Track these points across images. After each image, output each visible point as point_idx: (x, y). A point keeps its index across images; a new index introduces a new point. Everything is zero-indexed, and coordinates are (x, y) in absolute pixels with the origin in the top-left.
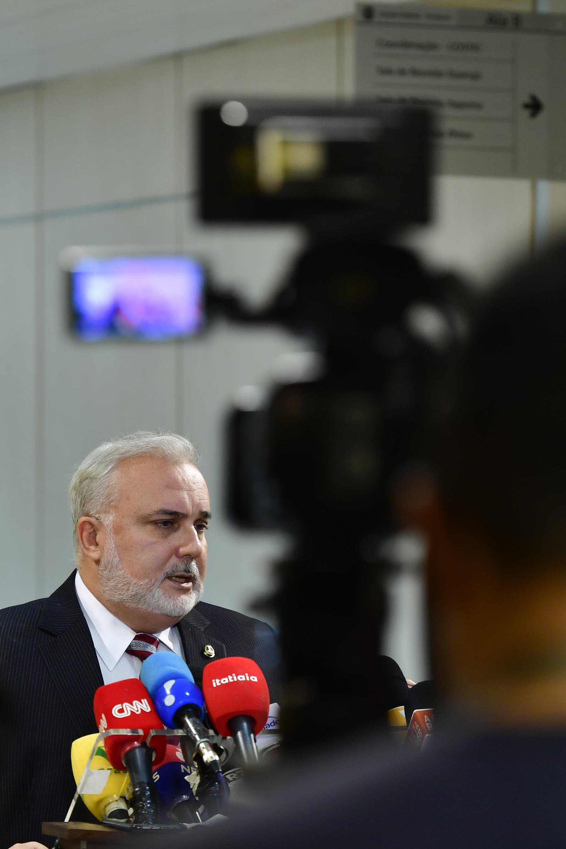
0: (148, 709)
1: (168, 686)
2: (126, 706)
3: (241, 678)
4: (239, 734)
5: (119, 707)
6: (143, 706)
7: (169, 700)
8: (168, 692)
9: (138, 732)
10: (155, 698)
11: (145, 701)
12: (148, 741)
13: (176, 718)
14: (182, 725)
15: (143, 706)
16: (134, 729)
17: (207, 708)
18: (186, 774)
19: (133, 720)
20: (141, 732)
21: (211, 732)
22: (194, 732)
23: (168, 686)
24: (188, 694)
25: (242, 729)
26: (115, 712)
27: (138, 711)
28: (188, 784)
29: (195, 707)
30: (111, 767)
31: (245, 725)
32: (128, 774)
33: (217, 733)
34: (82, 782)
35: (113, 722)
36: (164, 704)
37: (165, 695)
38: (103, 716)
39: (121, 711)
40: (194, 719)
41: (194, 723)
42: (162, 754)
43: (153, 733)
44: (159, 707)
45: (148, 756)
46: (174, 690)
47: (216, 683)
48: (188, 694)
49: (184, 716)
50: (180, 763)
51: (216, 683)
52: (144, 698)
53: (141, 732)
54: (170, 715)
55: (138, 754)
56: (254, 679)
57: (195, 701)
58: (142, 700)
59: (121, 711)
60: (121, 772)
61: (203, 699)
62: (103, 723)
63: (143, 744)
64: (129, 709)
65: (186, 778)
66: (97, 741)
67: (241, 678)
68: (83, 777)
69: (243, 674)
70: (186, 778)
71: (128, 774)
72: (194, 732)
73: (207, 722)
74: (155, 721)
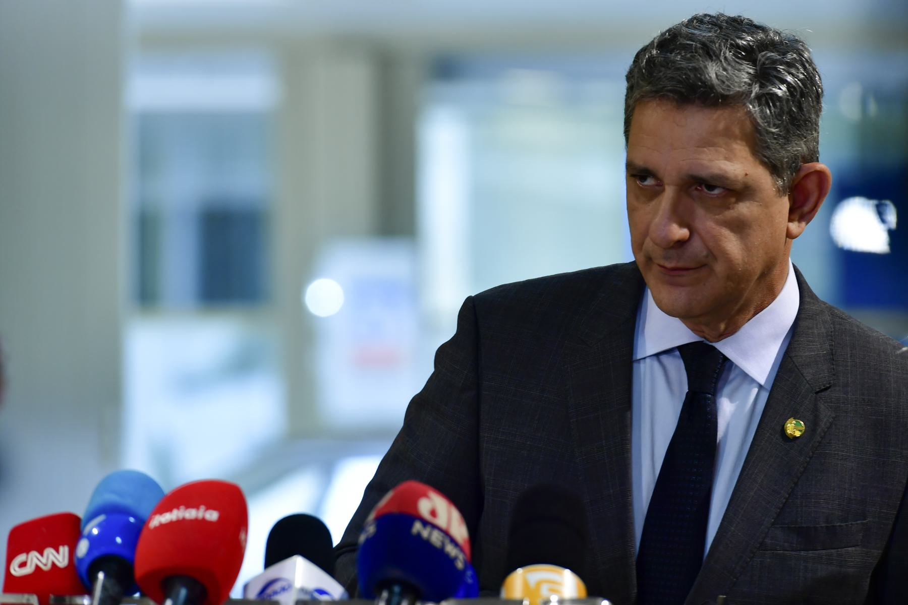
2: (34, 554)
3: (191, 514)
5: (21, 558)
11: (64, 550)
24: (119, 540)
27: (45, 565)
31: (183, 592)
39: (23, 565)
41: (104, 587)
48: (119, 540)
52: (63, 545)
56: (212, 516)
58: (61, 549)
59: (23, 565)
64: (35, 561)
67: (191, 514)
69: (197, 507)
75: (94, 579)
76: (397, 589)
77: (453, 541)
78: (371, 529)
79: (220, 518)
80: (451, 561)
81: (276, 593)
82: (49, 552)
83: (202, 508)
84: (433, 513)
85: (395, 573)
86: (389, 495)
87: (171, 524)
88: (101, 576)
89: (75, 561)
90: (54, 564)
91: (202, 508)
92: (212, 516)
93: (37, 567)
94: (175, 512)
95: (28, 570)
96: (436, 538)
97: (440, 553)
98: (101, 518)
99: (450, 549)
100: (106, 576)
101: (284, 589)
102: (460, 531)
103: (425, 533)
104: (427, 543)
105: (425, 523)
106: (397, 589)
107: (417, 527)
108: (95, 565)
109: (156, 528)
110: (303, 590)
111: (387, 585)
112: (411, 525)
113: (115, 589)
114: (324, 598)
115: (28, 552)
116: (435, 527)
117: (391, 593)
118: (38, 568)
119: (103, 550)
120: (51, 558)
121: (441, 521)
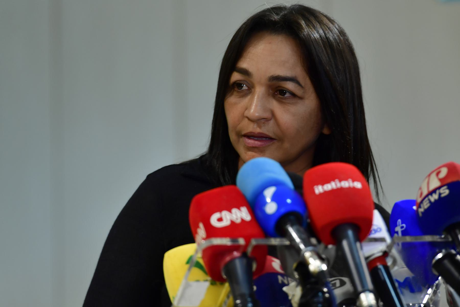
0: (247, 217)
6: (242, 214)
7: (271, 208)
8: (268, 200)
9: (237, 241)
12: (250, 250)
13: (278, 226)
15: (242, 214)
16: (234, 238)
17: (310, 216)
18: (284, 285)
19: (233, 230)
20: (242, 241)
21: (314, 241)
22: (297, 240)
23: (269, 193)
24: (289, 201)
25: (347, 237)
26: (214, 220)
27: (237, 219)
28: (286, 295)
29: (299, 214)
30: (209, 278)
31: (350, 233)
32: (227, 285)
33: (319, 241)
34: (179, 294)
35: (212, 232)
36: (264, 212)
37: (265, 203)
38: (201, 225)
39: (220, 220)
40: (296, 227)
42: (262, 264)
43: (254, 242)
44: (259, 214)
45: (248, 267)
46: (275, 198)
47: (319, 189)
48: (289, 201)
49: (286, 224)
50: (278, 273)
51: (319, 189)
52: (243, 206)
53: (242, 241)
54: (272, 224)
57: (298, 209)
59: (220, 220)
60: (218, 283)
61: (305, 205)
62: (201, 232)
63: (244, 255)
65: (285, 289)
66: (197, 252)
67: (345, 184)
68: (181, 289)
69: (346, 179)
70: (285, 289)
71: (227, 285)
72: (297, 240)
73: (310, 231)
74: (256, 230)
78: (445, 192)
82: (234, 210)
93: (233, 223)
95: (226, 223)
100: (292, 226)
109: (321, 194)
118: (233, 223)
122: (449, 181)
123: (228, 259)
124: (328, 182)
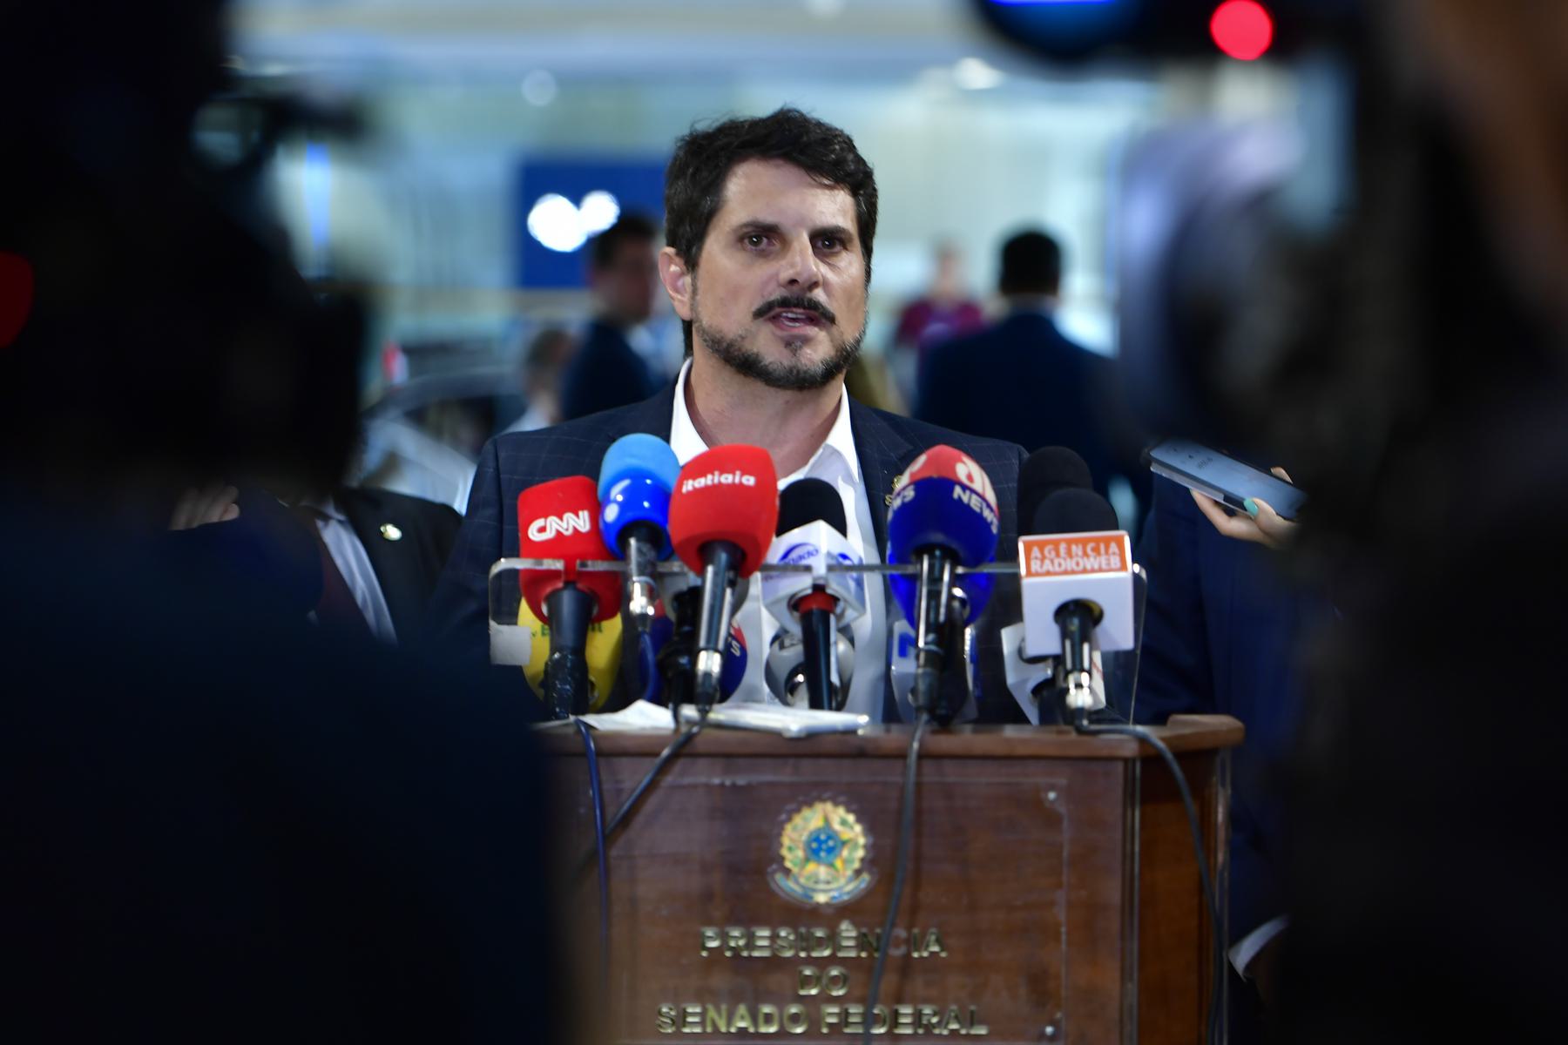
1: (617, 494)
3: (727, 479)
4: (710, 569)
5: (539, 523)
7: (611, 513)
10: (597, 511)
14: (621, 554)
19: (557, 546)
24: (646, 504)
31: (723, 557)
39: (542, 530)
41: (639, 551)
48: (646, 504)
55: (567, 601)
56: (749, 481)
57: (657, 516)
59: (542, 530)
64: (555, 526)
67: (727, 479)
75: (626, 545)
76: (938, 553)
77: (989, 506)
78: (910, 494)
79: (758, 482)
80: (988, 525)
81: (801, 557)
82: (569, 516)
83: (738, 473)
84: (970, 477)
85: (938, 537)
86: (922, 459)
87: (706, 488)
88: (633, 542)
89: (601, 525)
90: (575, 530)
91: (738, 473)
92: (749, 481)
93: (559, 533)
94: (710, 477)
95: (549, 535)
96: (975, 503)
97: (979, 517)
98: (625, 483)
99: (987, 514)
100: (638, 540)
101: (810, 554)
102: (991, 496)
103: (965, 499)
104: (968, 507)
105: (965, 488)
106: (938, 553)
107: (958, 491)
108: (625, 529)
109: (689, 493)
110: (829, 554)
111: (929, 549)
112: (952, 490)
113: (652, 554)
114: (847, 562)
115: (546, 517)
116: (973, 491)
117: (932, 557)
118: (559, 533)
119: (630, 515)
120: (572, 523)
121: (977, 486)
122: (919, 477)
123: (549, 590)
124: (704, 475)
